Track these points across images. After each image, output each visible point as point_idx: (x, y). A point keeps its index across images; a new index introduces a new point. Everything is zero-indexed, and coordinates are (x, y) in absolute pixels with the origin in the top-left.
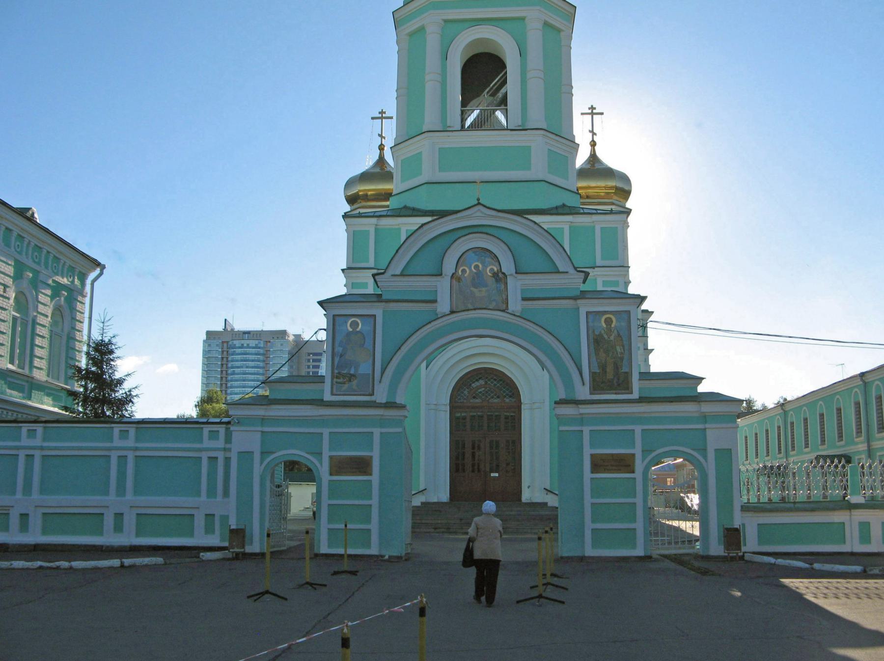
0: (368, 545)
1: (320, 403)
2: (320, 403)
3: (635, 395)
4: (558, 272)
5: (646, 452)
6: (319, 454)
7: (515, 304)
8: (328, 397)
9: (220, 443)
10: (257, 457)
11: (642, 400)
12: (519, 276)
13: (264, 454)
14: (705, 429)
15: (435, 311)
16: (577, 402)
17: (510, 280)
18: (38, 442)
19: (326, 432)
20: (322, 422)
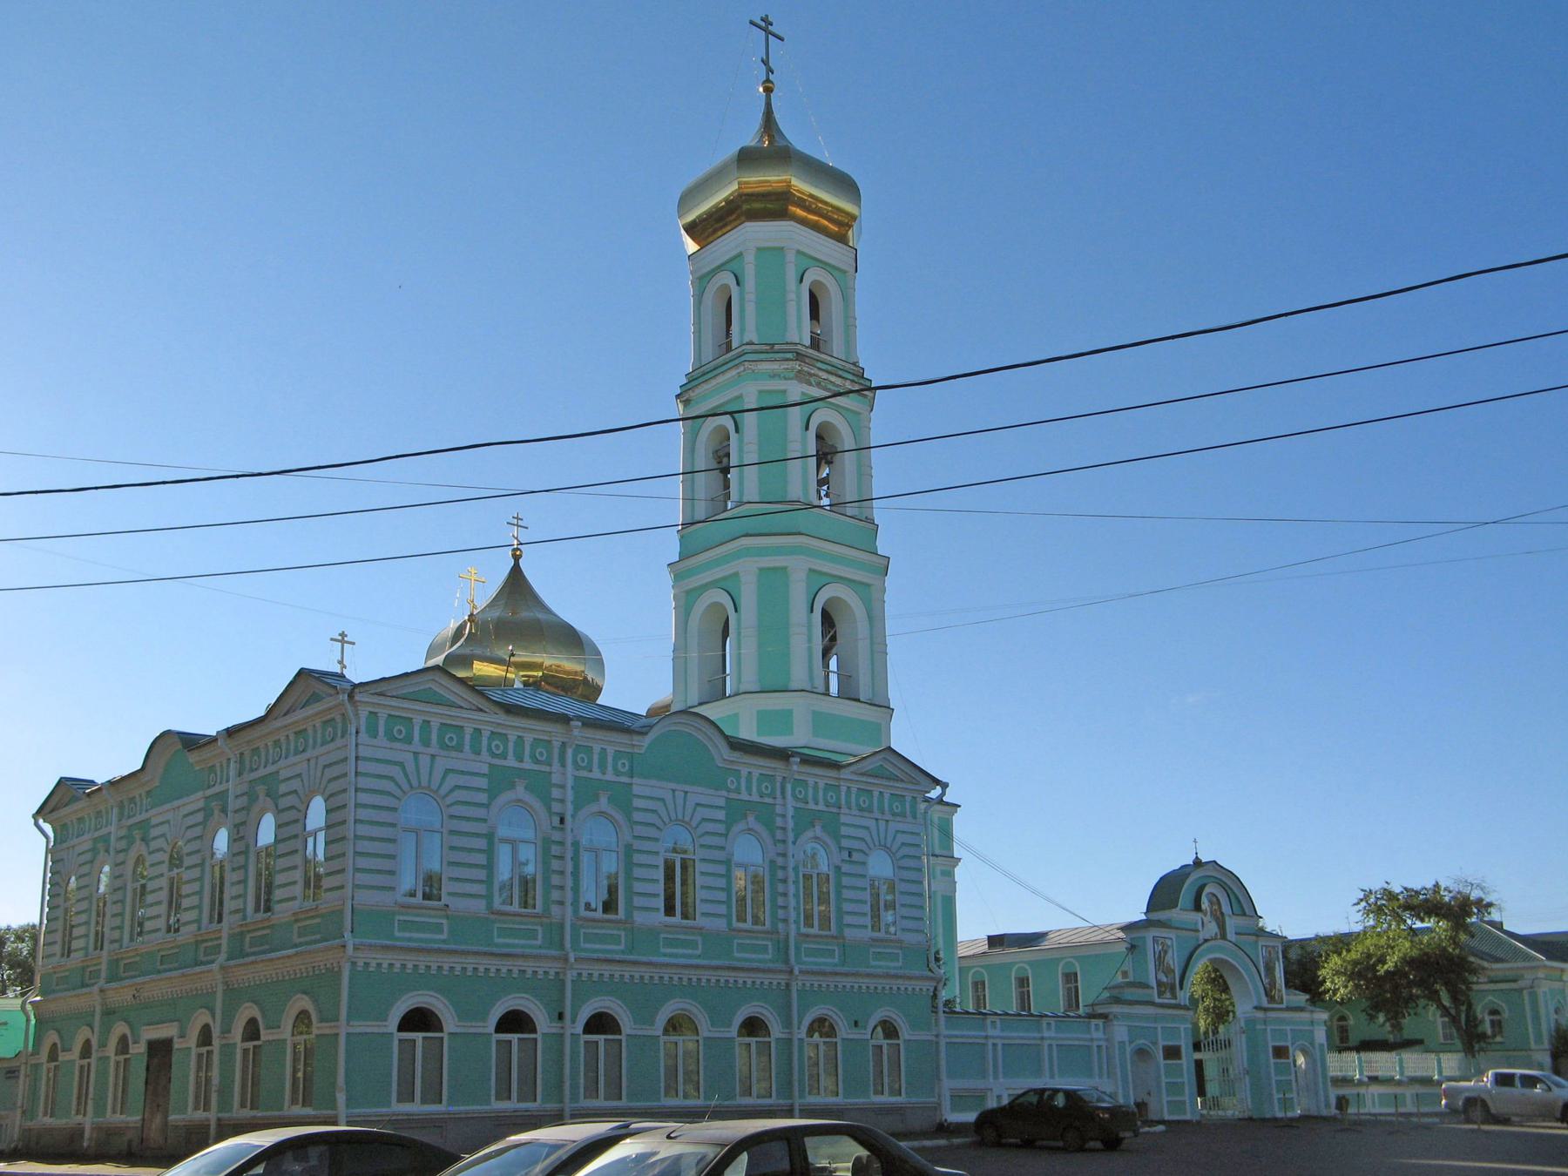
0: (1185, 1113)
1: (1152, 1004)
2: (1152, 1004)
3: (1284, 1006)
4: (1244, 914)
5: (1293, 1044)
6: (1155, 1043)
7: (1231, 935)
8: (1157, 1000)
9: (1100, 1035)
10: (1127, 1043)
11: (1288, 1009)
12: (1234, 917)
13: (1131, 1042)
14: (1312, 1031)
15: (1198, 940)
16: (1266, 1010)
17: (1227, 919)
18: (997, 1032)
19: (1159, 1026)
20: (1156, 1019)
